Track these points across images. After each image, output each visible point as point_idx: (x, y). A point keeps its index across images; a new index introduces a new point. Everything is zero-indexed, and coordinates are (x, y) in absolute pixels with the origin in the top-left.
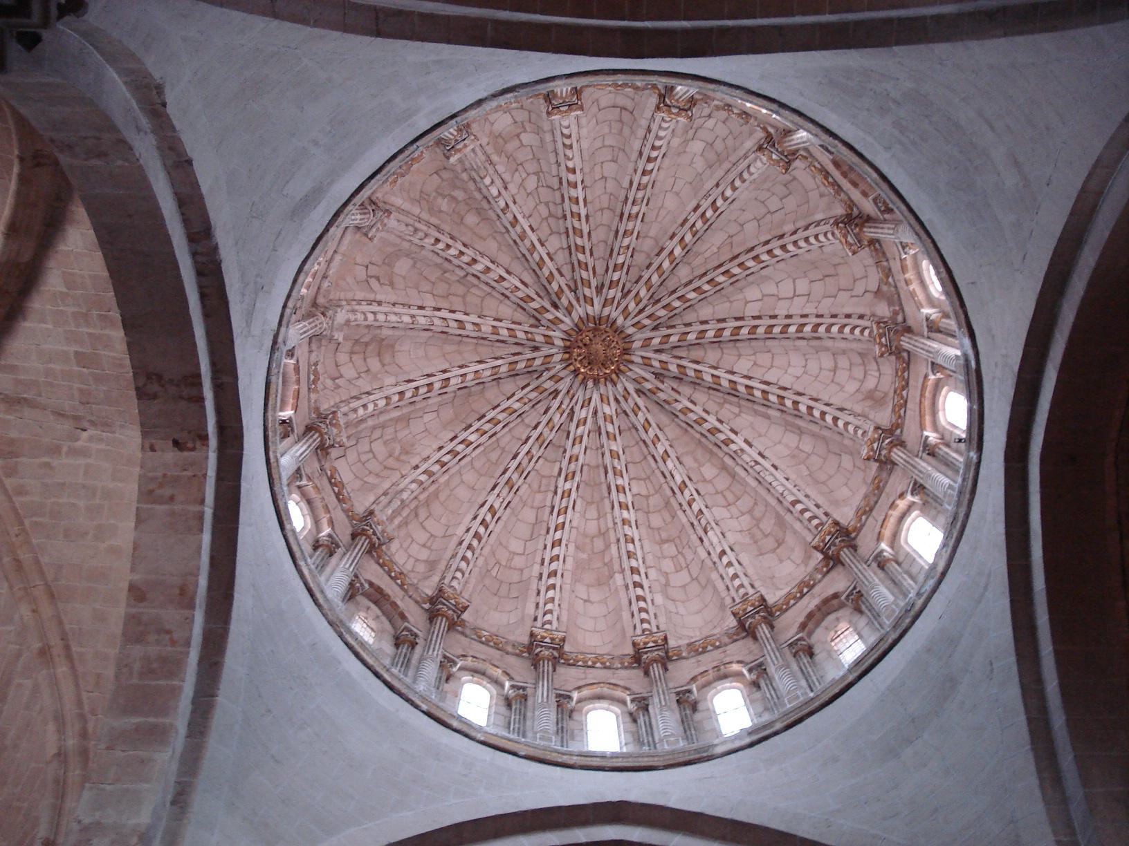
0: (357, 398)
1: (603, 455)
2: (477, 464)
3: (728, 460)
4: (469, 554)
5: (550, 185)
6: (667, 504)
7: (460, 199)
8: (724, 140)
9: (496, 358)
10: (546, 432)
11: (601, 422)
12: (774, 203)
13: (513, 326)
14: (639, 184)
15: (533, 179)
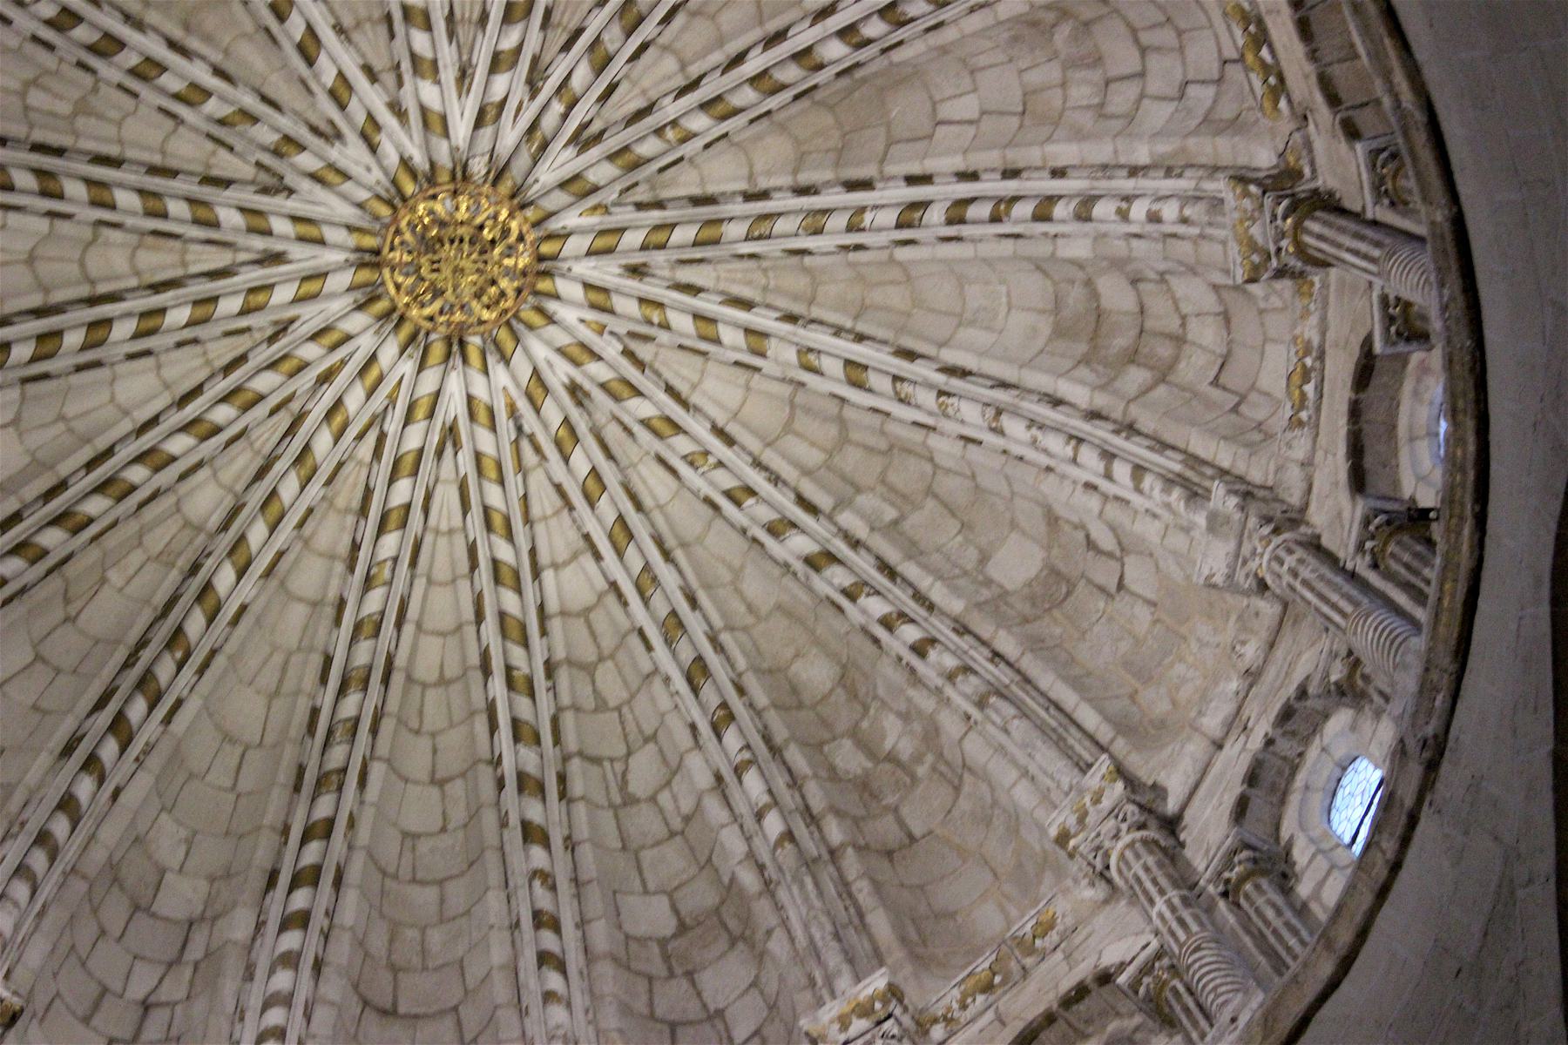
5: (594, 770)
7: (847, 744)
8: (103, 932)
9: (752, 256)
10: (612, 38)
11: (448, 57)
13: (703, 346)
14: (340, 789)
15: (637, 786)
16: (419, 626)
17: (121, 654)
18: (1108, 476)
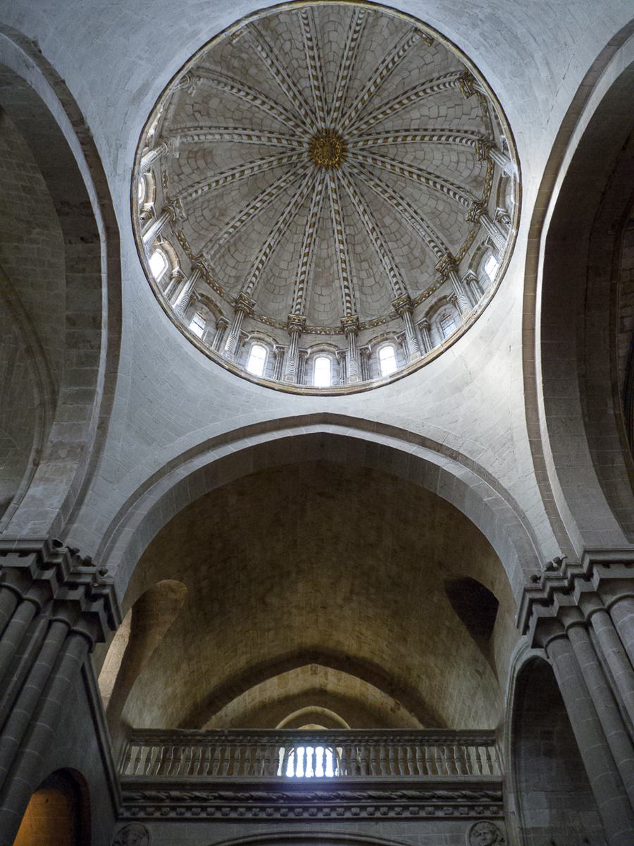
0: (192, 186)
1: (331, 211)
2: (262, 220)
3: (397, 214)
4: (257, 273)
6: (365, 239)
7: (245, 58)
9: (271, 156)
11: (330, 192)
12: (428, 58)
16: (334, 73)
17: (393, 73)
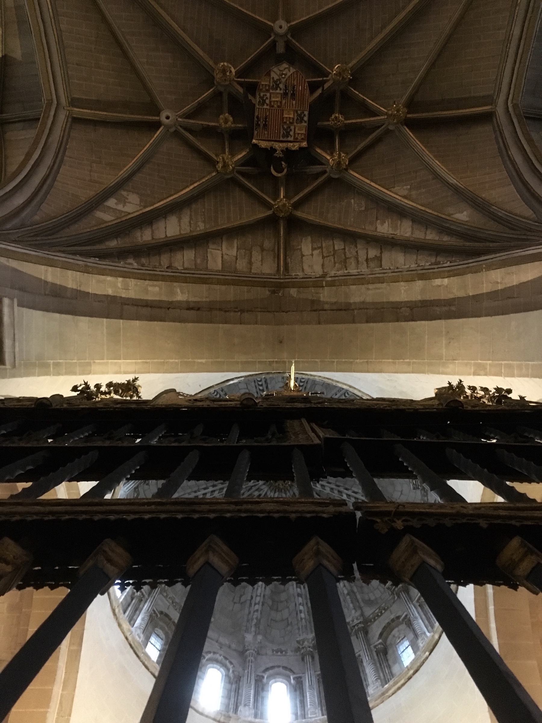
18: (255, 604)
